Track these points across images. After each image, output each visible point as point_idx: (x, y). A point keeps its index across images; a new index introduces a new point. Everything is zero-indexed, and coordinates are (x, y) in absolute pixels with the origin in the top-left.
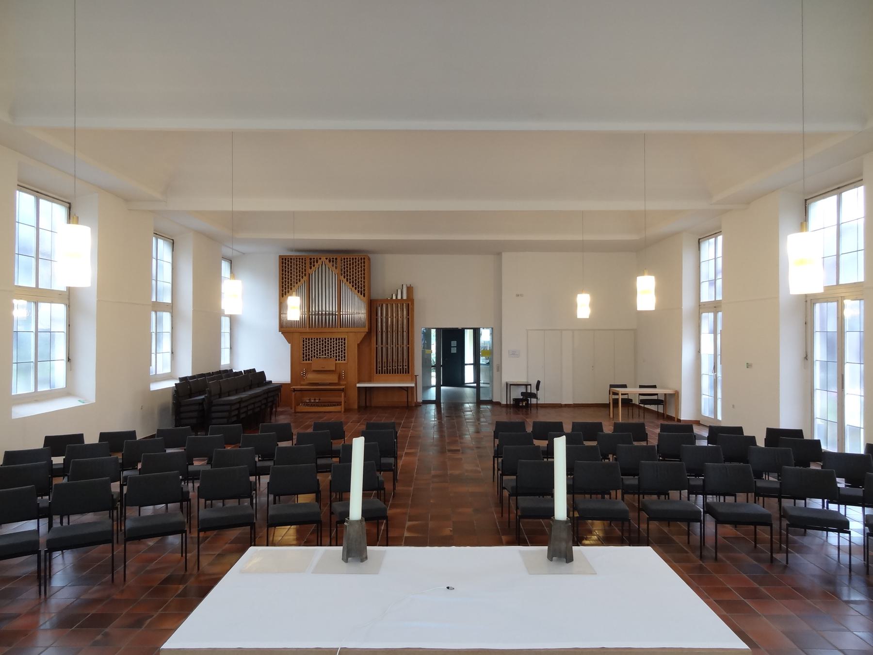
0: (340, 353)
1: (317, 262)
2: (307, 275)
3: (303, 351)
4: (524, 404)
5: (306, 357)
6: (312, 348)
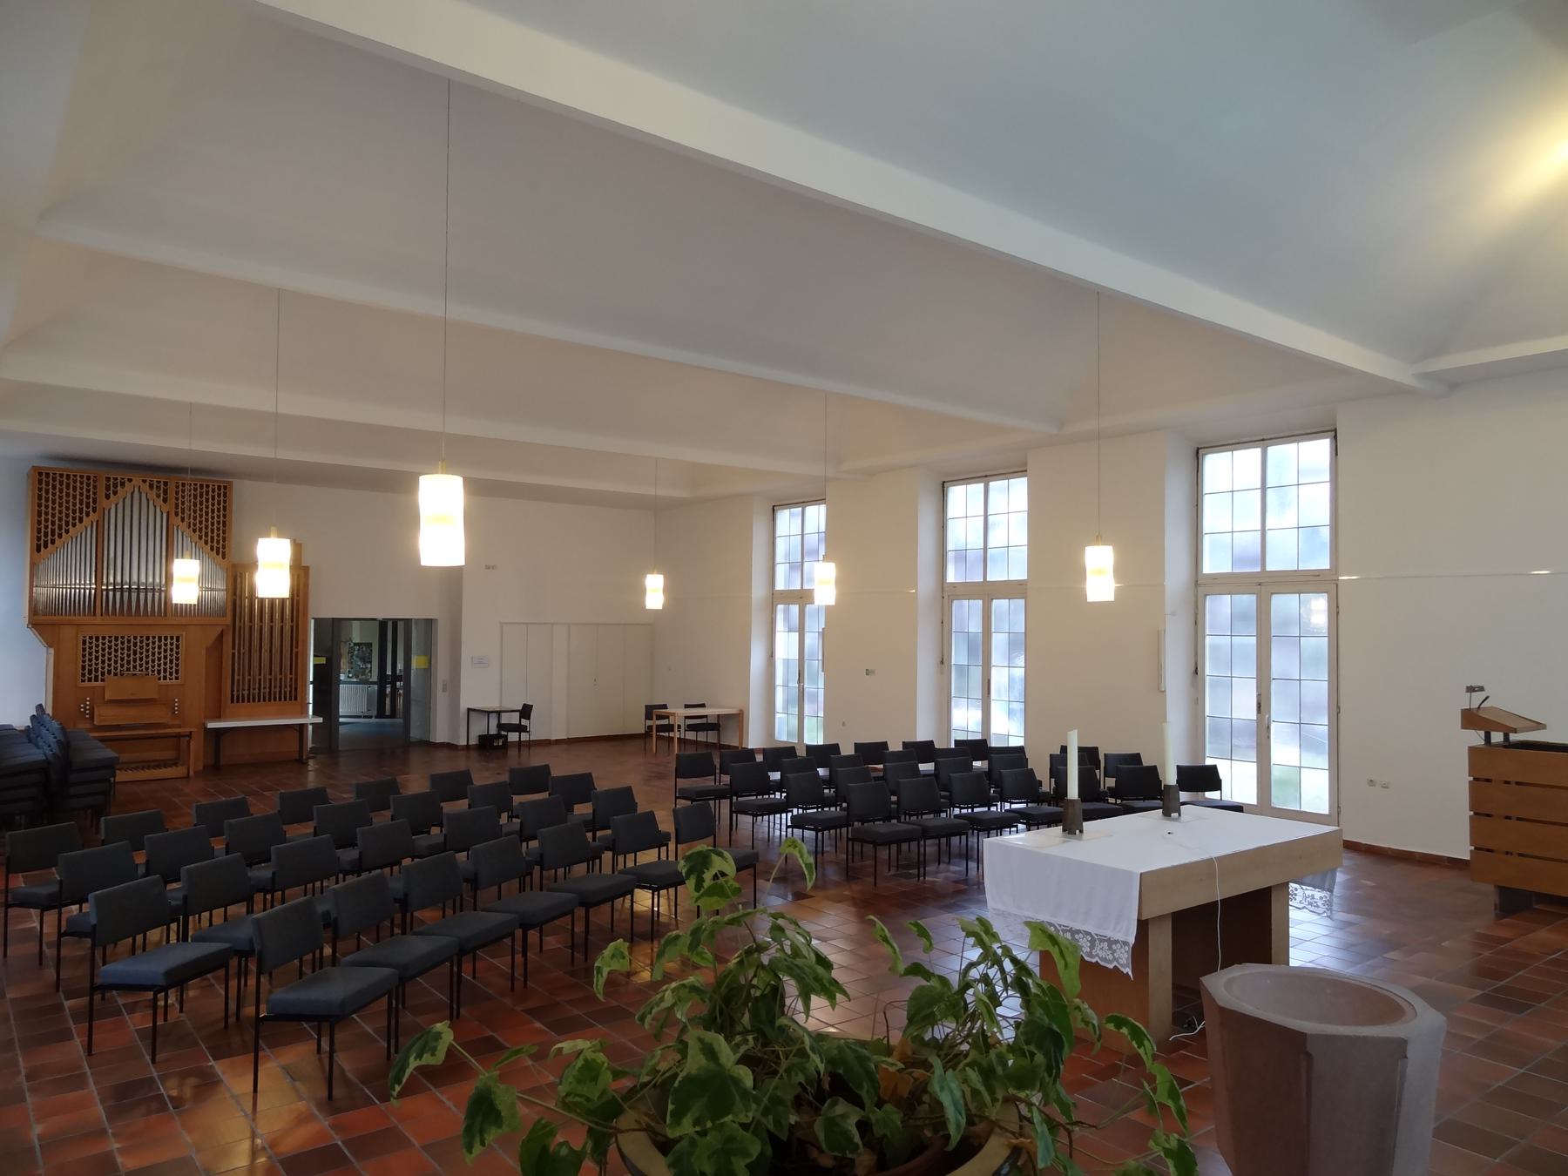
0: (168, 665)
1: (123, 484)
4: (500, 744)
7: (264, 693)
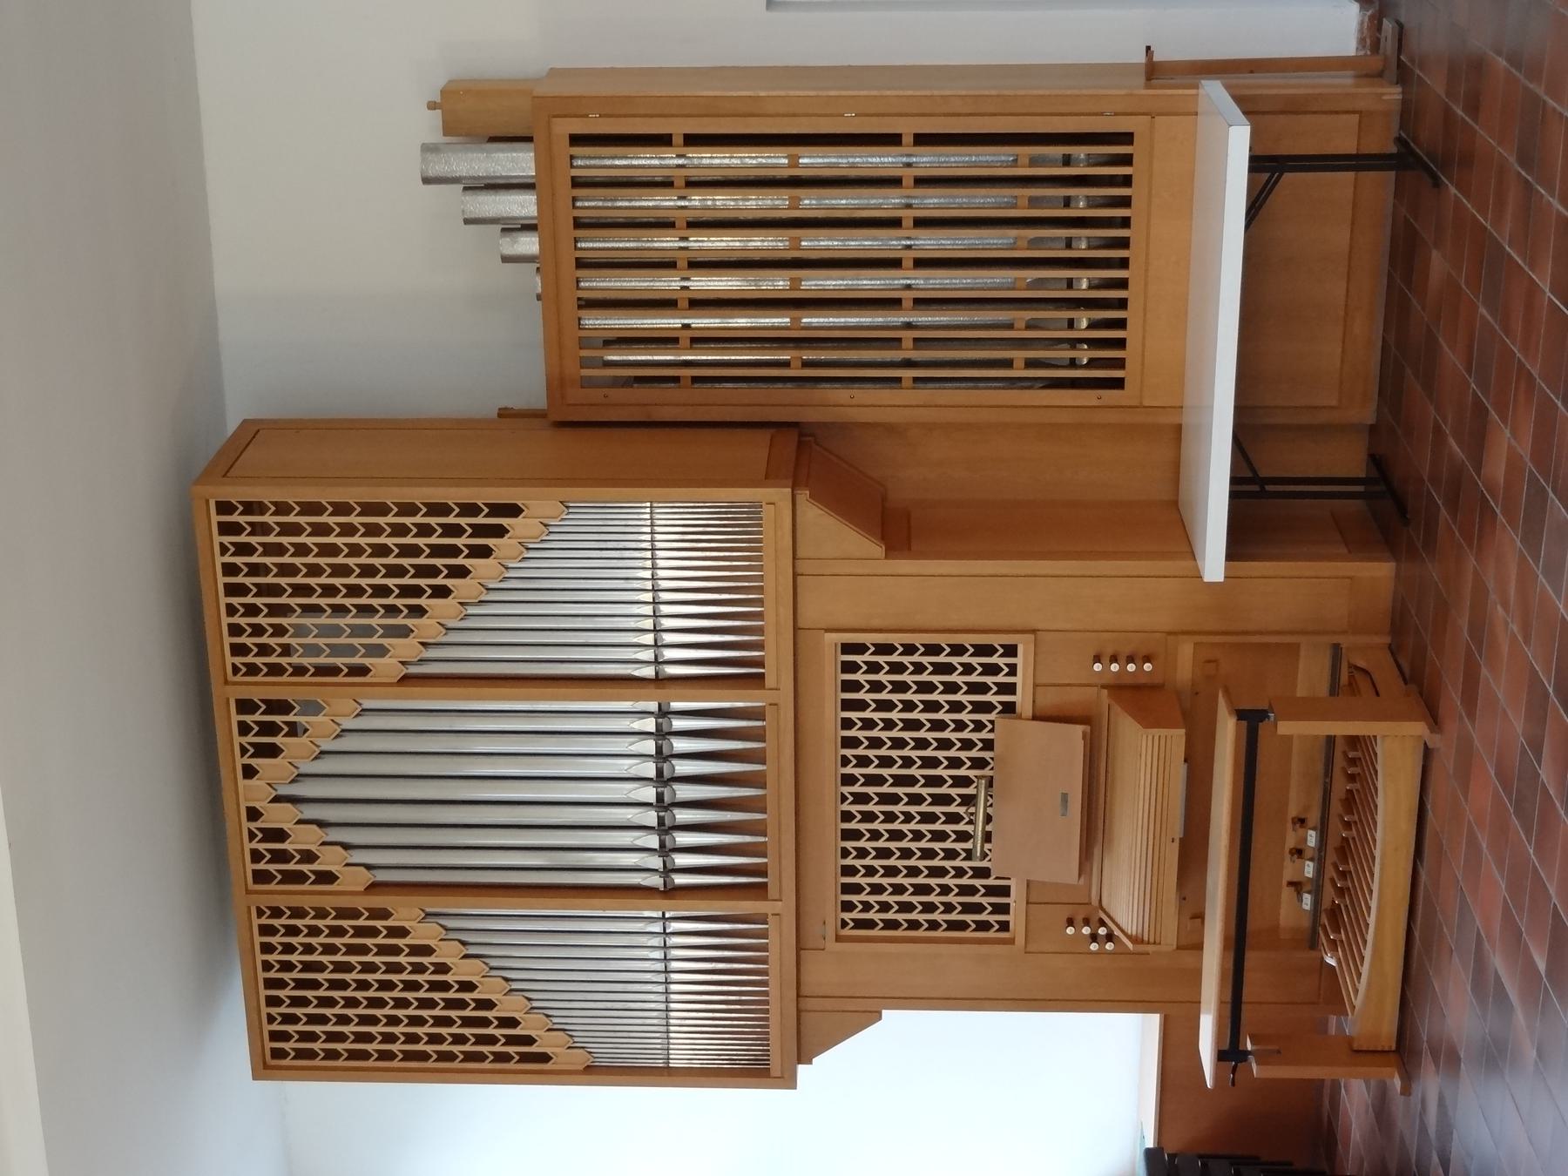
1: (279, 835)
2: (378, 901)
3: (934, 925)
6: (913, 872)
7: (1093, 203)
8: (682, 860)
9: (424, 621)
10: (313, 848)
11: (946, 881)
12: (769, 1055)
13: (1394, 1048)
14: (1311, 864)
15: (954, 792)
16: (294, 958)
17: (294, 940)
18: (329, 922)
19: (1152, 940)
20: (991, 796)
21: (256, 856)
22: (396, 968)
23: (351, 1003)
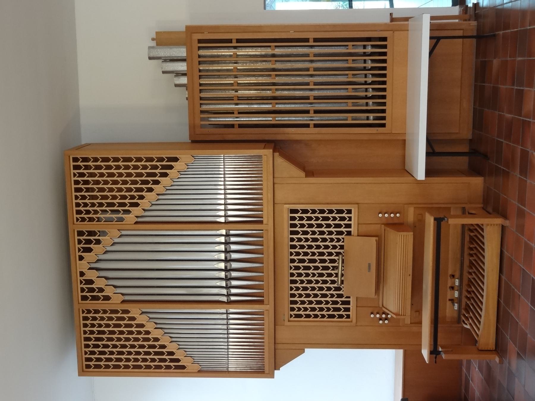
1: (91, 282)
2: (126, 307)
3: (323, 316)
5: (339, 310)
6: (316, 296)
8: (233, 291)
9: (144, 201)
10: (103, 287)
11: (328, 299)
12: (264, 366)
13: (494, 349)
14: (457, 292)
15: (330, 265)
16: (95, 329)
17: (95, 322)
18: (108, 315)
19: (403, 314)
20: (343, 266)
21: (83, 290)
22: (131, 333)
23: (115, 346)
